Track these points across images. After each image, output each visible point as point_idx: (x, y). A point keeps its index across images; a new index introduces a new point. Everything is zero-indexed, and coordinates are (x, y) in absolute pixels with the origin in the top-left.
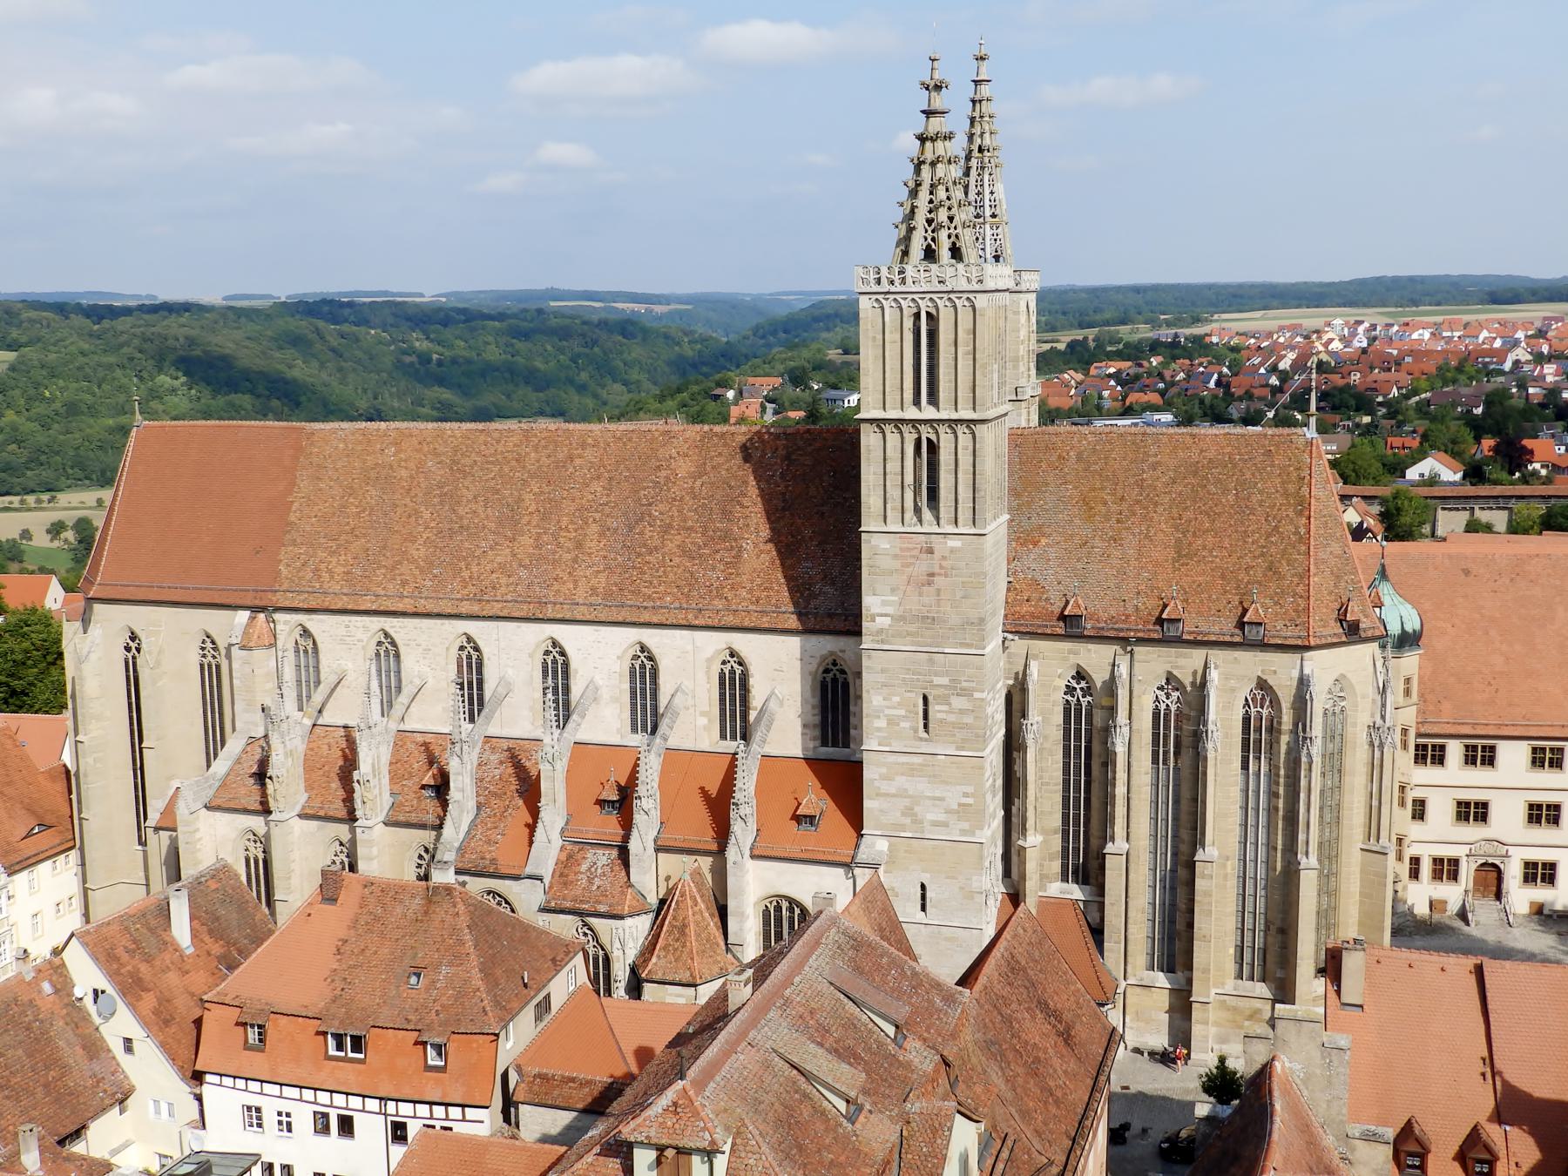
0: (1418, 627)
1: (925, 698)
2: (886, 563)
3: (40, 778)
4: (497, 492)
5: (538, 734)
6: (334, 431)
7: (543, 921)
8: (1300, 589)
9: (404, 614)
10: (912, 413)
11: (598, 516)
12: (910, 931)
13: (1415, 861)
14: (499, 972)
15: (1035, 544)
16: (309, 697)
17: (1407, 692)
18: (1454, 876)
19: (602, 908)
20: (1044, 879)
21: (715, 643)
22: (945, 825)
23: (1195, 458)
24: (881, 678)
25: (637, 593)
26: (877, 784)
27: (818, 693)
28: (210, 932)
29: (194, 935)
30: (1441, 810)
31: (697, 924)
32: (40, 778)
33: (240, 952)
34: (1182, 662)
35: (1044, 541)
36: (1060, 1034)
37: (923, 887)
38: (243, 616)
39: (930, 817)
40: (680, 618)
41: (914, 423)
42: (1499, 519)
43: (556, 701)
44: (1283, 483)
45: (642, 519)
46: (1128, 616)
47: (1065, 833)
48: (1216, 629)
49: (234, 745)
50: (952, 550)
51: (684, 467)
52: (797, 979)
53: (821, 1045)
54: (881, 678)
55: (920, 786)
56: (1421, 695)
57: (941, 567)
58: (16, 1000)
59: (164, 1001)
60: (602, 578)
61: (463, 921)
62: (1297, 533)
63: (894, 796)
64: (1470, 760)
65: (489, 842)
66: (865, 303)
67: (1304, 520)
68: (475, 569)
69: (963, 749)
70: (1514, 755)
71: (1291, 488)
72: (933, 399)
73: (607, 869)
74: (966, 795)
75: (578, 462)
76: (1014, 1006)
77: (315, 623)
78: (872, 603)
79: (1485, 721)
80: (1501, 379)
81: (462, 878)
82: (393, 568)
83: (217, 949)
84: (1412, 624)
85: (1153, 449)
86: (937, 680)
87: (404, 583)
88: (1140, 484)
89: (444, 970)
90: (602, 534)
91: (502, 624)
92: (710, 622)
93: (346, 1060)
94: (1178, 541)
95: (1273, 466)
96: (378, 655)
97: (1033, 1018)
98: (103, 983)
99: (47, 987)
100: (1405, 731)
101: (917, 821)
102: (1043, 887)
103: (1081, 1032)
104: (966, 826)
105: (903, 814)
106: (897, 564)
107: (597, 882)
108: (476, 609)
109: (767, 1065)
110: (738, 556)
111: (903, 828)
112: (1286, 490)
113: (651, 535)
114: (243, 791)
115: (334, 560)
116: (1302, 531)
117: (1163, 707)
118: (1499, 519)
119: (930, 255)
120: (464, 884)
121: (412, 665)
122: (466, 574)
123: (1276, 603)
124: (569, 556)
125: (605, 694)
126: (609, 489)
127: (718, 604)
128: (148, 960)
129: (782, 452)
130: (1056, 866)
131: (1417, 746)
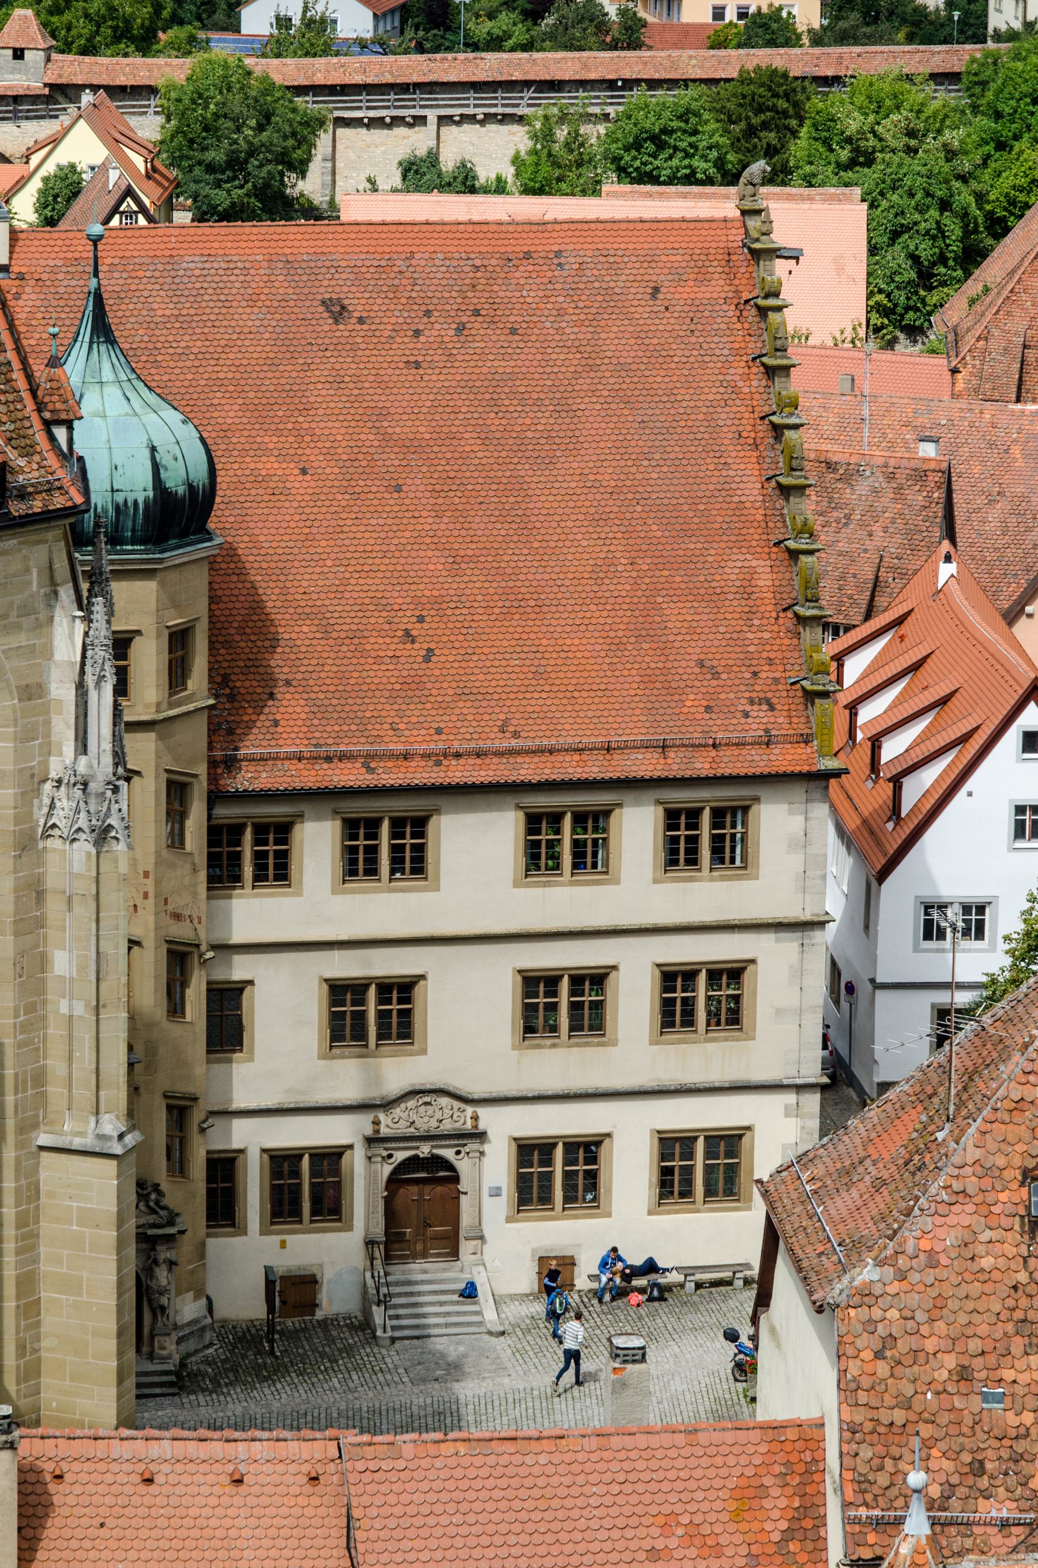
0: (199, 473)
17: (177, 673)
42: (493, 149)
84: (186, 464)
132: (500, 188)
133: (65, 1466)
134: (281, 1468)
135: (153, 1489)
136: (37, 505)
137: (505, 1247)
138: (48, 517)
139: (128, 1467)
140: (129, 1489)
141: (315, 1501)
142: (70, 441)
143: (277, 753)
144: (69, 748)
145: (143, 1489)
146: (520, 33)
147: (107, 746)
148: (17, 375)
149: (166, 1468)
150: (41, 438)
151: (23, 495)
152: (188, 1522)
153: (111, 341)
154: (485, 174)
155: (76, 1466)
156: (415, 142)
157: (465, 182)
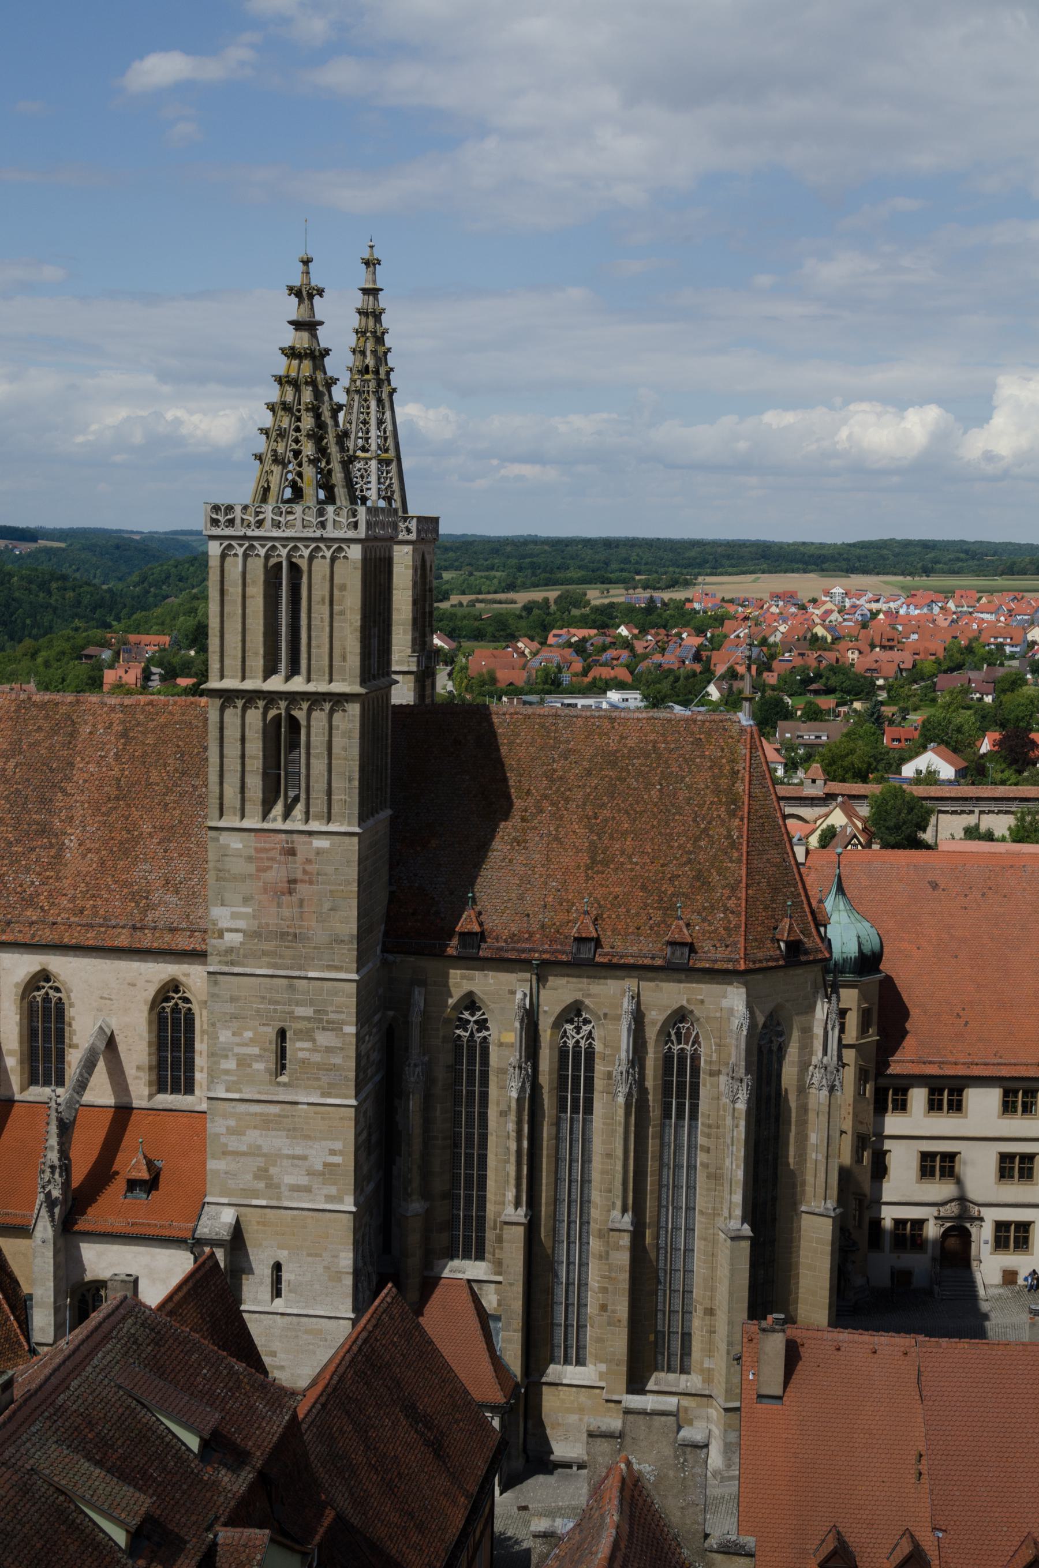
0: (877, 947)
1: (282, 1034)
2: (238, 866)
8: (731, 903)
10: (276, 683)
22: (307, 1189)
23: (613, 746)
24: (230, 1008)
26: (223, 1140)
27: (155, 1027)
37: (277, 1267)
39: (289, 1180)
41: (271, 698)
42: (1001, 824)
44: (714, 777)
46: (531, 934)
50: (319, 852)
52: (74, 1384)
53: (99, 1464)
54: (230, 1008)
55: (276, 1142)
57: (305, 872)
62: (729, 836)
63: (244, 1154)
66: (214, 549)
67: (737, 822)
71: (724, 783)
74: (333, 1152)
78: (221, 915)
80: (1015, 663)
84: (872, 942)
85: (566, 735)
92: (20, 938)
94: (592, 843)
95: (702, 756)
101: (273, 1186)
104: (333, 1190)
105: (256, 1177)
106: (251, 868)
110: (59, 856)
111: (256, 1194)
112: (718, 786)
117: (571, 1043)
118: (1001, 824)
119: (298, 493)
123: (704, 920)
129: (117, 728)
132: (1003, 839)
133: (805, 1341)
134: (892, 1348)
135: (840, 1353)
136: (811, 958)
138: (815, 961)
139: (830, 1343)
140: (830, 1352)
141: (905, 1363)
142: (825, 932)
144: (820, 1054)
145: (836, 1353)
146: (1014, 779)
147: (835, 1053)
148: (805, 906)
149: (845, 1345)
150: (813, 930)
151: (807, 952)
152: (853, 1368)
153: (844, 894)
154: (997, 834)
155: (809, 1341)
156: (971, 820)
157: (989, 837)
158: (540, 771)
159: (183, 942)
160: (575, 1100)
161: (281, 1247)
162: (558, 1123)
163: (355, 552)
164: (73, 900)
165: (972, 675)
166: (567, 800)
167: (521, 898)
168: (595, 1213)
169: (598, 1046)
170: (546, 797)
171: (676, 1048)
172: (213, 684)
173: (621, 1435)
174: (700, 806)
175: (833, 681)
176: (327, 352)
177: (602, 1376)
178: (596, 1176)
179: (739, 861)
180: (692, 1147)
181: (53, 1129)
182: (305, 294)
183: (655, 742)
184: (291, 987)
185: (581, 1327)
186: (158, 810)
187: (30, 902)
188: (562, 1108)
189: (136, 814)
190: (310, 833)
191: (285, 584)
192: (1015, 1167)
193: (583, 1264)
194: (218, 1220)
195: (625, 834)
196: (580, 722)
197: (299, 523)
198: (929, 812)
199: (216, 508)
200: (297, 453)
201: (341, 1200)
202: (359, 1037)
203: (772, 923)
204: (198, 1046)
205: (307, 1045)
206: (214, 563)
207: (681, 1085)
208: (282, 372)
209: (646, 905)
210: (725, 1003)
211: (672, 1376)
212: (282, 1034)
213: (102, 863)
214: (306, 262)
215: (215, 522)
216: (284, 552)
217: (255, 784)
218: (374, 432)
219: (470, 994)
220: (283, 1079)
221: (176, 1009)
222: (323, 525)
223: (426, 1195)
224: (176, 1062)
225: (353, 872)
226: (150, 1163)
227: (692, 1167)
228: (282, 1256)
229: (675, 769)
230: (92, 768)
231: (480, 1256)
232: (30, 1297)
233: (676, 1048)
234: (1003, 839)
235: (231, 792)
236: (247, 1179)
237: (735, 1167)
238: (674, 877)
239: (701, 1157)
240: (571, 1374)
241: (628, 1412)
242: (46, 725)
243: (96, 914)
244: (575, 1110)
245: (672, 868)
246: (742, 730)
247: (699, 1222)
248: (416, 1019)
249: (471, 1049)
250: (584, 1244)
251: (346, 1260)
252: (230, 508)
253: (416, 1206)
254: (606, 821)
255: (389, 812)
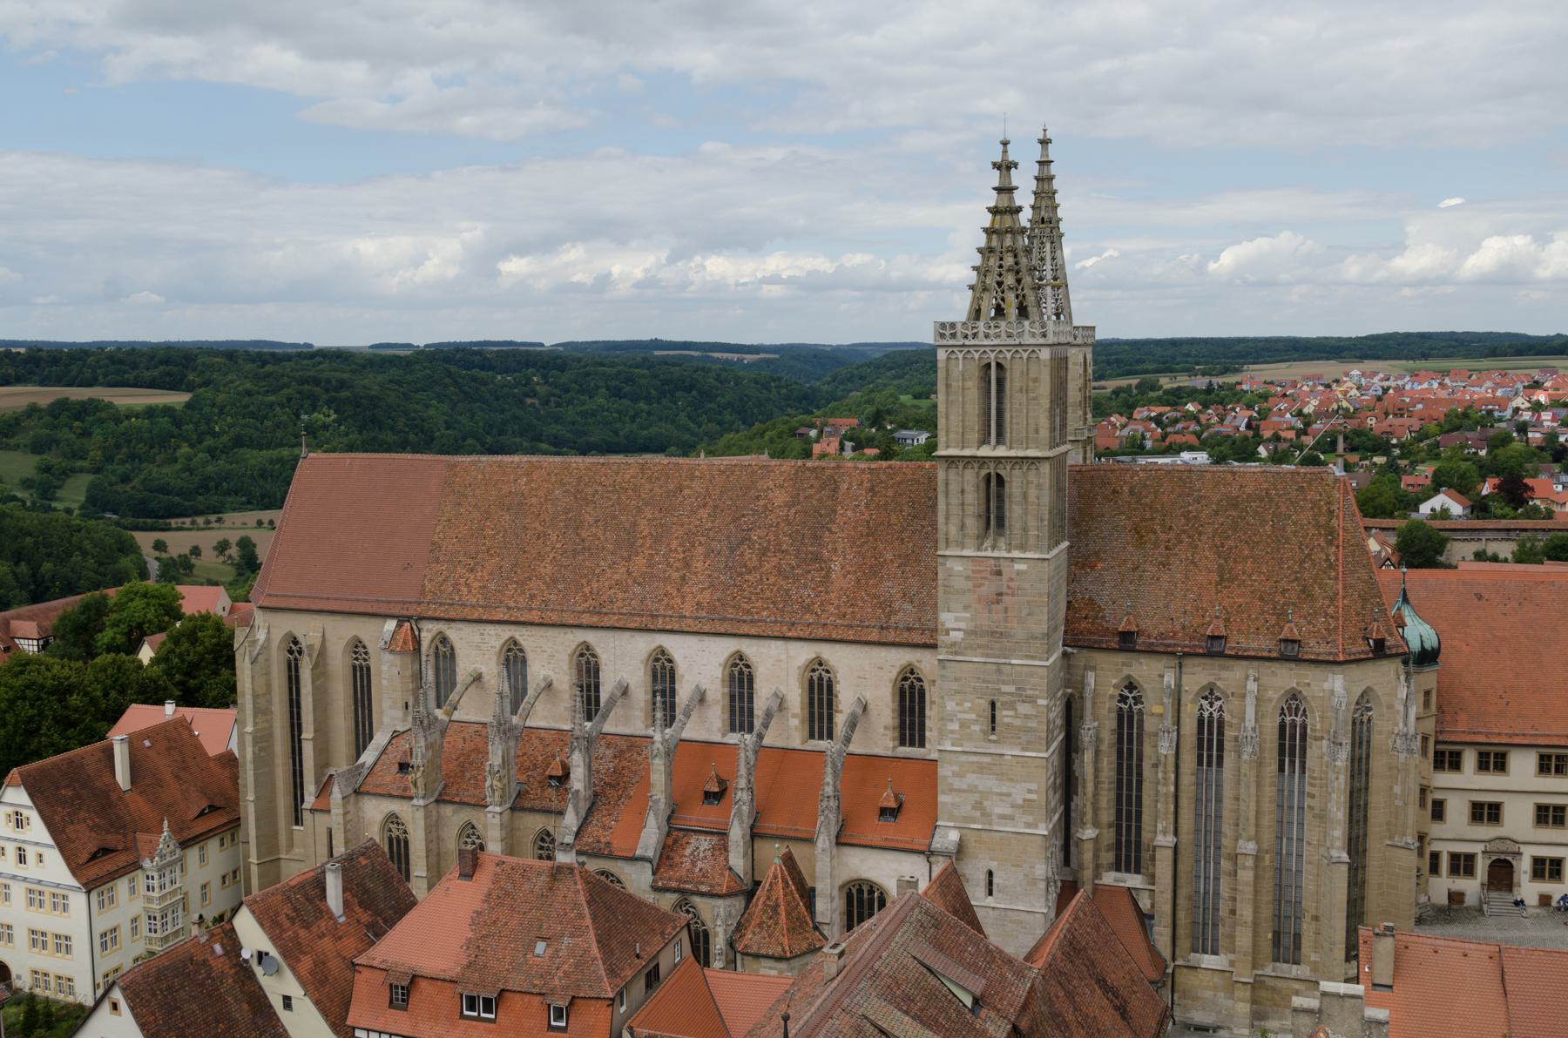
0: (1436, 644)
1: (993, 705)
2: (959, 583)
3: (212, 764)
4: (614, 517)
5: (650, 732)
6: (474, 463)
7: (650, 897)
8: (1330, 611)
9: (532, 624)
10: (985, 451)
11: (703, 539)
12: (980, 914)
13: (1435, 856)
14: (614, 944)
15: (1092, 568)
16: (447, 697)
18: (1469, 871)
19: (704, 888)
20: (1098, 869)
21: (802, 653)
22: (1011, 818)
23: (1235, 493)
24: (954, 686)
25: (737, 608)
28: (361, 904)
29: (347, 904)
30: (1457, 810)
31: (788, 904)
32: (212, 764)
33: (385, 921)
34: (1224, 674)
35: (1100, 566)
36: (1116, 1008)
37: (990, 873)
38: (391, 625)
39: (998, 810)
40: (776, 630)
41: (982, 461)
42: (1505, 549)
43: (664, 703)
45: (742, 543)
47: (1119, 832)
48: (1255, 645)
49: (380, 739)
50: (1019, 573)
51: (780, 498)
53: (906, 1013)
54: (954, 686)
55: (988, 783)
56: (1440, 707)
58: (191, 960)
59: (320, 964)
60: (707, 594)
61: (582, 899)
62: (1327, 560)
64: (1483, 766)
65: (604, 828)
66: (942, 355)
67: (1334, 549)
68: (595, 585)
69: (1026, 749)
70: (1523, 765)
71: (1322, 520)
72: (1000, 438)
73: (709, 854)
74: (1030, 791)
75: (687, 492)
76: (1075, 982)
77: (455, 633)
78: (947, 618)
79: (1498, 731)
80: (1503, 425)
81: (582, 859)
82: (524, 584)
83: (366, 917)
84: (1431, 641)
85: (1198, 485)
86: (1005, 688)
87: (532, 597)
88: (1186, 515)
89: (566, 941)
90: (707, 556)
91: (617, 634)
92: (801, 634)
93: (479, 1019)
94: (1220, 566)
96: (507, 660)
97: (1093, 991)
98: (267, 945)
99: (218, 948)
100: (1425, 739)
101: (986, 815)
102: (1097, 875)
103: (1136, 1005)
104: (1030, 819)
105: (974, 808)
106: (970, 585)
107: (699, 864)
108: (595, 620)
109: (859, 1030)
110: (827, 576)
113: (751, 557)
114: (389, 779)
115: (472, 576)
116: (1332, 558)
117: (1206, 714)
118: (1505, 549)
119: (1000, 311)
120: (583, 864)
121: (538, 670)
122: (587, 590)
124: (676, 575)
125: (710, 696)
126: (713, 516)
127: (809, 618)
128: (307, 926)
129: (866, 485)
130: (1108, 857)
131: (1436, 753)
132: (1506, 561)
137: (1529, 889)
138: (1397, 655)
143: (1460, 728)
146: (1512, 513)
154: (1502, 556)
157: (1495, 559)
158: (1178, 512)
159: (917, 638)
160: (1210, 756)
161: (992, 859)
162: (1197, 773)
163: (1045, 354)
164: (838, 607)
165: (1469, 434)
166: (1200, 533)
167: (1167, 606)
168: (1226, 842)
169: (1227, 717)
170: (1185, 532)
171: (1288, 719)
172: (941, 452)
173: (1320, 1011)
174: (1305, 537)
175: (1357, 441)
176: (1019, 209)
177: (1232, 963)
178: (1226, 814)
179: (1336, 578)
180: (1302, 792)
181: (829, 770)
182: (1005, 167)
183: (1267, 490)
184: (999, 671)
185: (1215, 925)
186: (897, 543)
187: (808, 609)
188: (1200, 763)
189: (881, 546)
190: (1012, 560)
191: (994, 378)
192: (1548, 815)
193: (1217, 879)
194: (948, 837)
195: (1245, 559)
196: (1209, 476)
197: (1003, 335)
198: (1446, 540)
199: (943, 325)
200: (1000, 284)
201: (1036, 827)
202: (1049, 709)
203: (1363, 625)
204: (928, 712)
205: (1012, 713)
206: (941, 365)
207: (1292, 747)
208: (988, 225)
209: (1263, 612)
210: (1327, 686)
211: (1285, 966)
212: (993, 705)
213: (858, 581)
214: (1005, 144)
215: (942, 336)
216: (992, 356)
217: (972, 525)
218: (1048, 267)
219: (1129, 677)
220: (993, 737)
221: (912, 687)
222: (1020, 334)
223: (1096, 824)
224: (912, 723)
225: (1044, 588)
226: (896, 796)
227: (1301, 808)
228: (993, 865)
229: (1283, 509)
230: (849, 513)
231: (1138, 871)
232: (813, 890)
233: (1288, 719)
234: (1506, 561)
235: (953, 530)
236: (967, 809)
237: (1338, 812)
238: (1285, 590)
239: (1308, 802)
240: (1208, 961)
241: (1324, 994)
242: (816, 484)
243: (854, 618)
244: (1209, 764)
245: (1283, 584)
246: (1337, 480)
247: (1307, 850)
248: (1088, 695)
249: (1131, 718)
250: (1217, 863)
251: (1041, 870)
252: (953, 325)
253: (1089, 833)
254: (1230, 549)
255: (1066, 544)
